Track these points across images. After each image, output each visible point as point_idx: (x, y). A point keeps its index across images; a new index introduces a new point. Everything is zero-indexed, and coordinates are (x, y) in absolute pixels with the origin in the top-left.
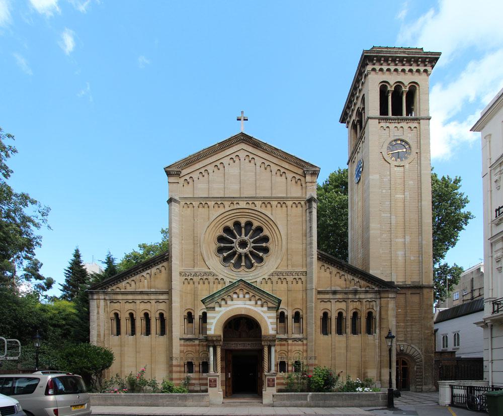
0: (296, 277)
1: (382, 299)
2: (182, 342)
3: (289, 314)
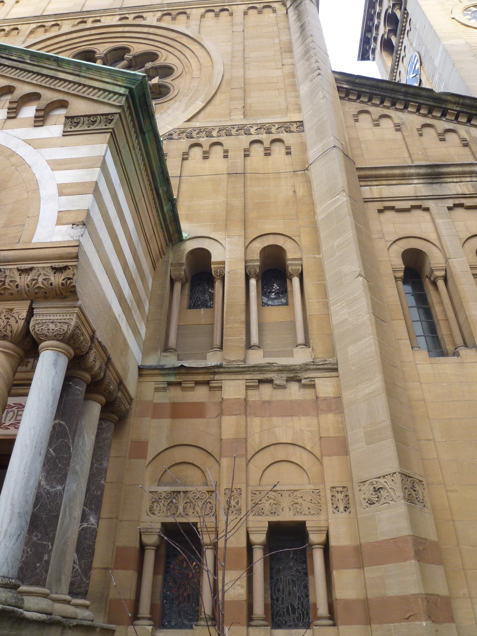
0: (263, 137)
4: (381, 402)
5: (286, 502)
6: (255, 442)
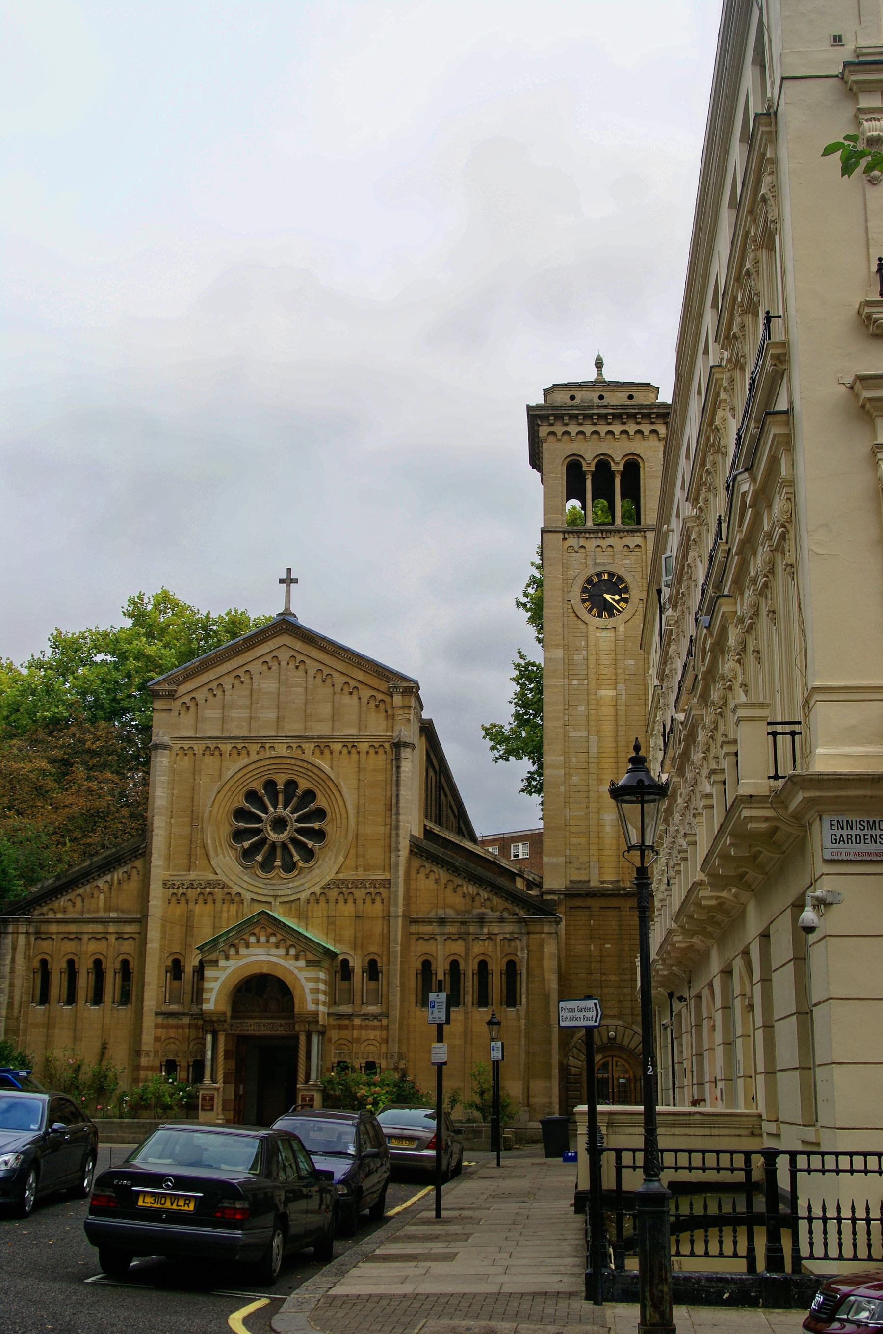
0: (372, 890)
2: (160, 1020)
3: (357, 963)
5: (371, 1056)
6: (363, 1038)
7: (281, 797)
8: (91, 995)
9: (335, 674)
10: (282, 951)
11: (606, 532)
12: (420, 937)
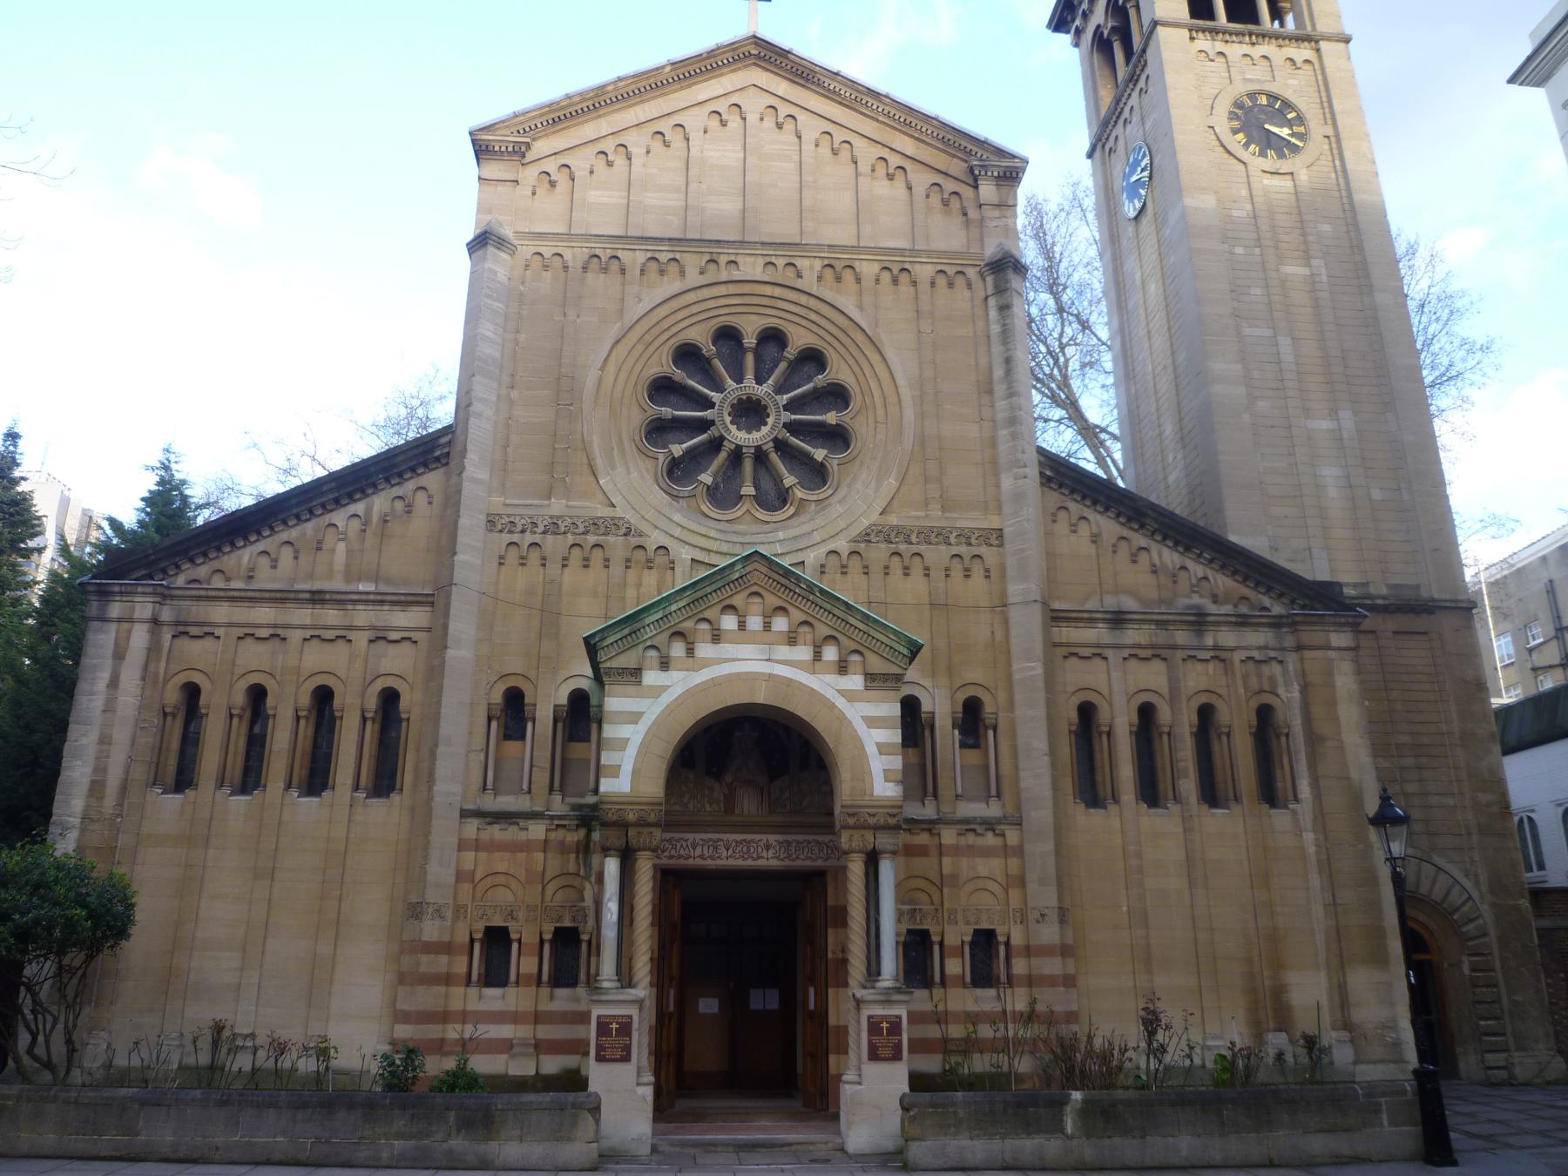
0: (963, 550)
1: (1308, 654)
2: (471, 828)
3: (940, 705)
4: (1051, 860)
7: (750, 359)
8: (300, 772)
9: (858, 142)
10: (803, 653)
11: (1257, 35)
12: (1072, 652)
